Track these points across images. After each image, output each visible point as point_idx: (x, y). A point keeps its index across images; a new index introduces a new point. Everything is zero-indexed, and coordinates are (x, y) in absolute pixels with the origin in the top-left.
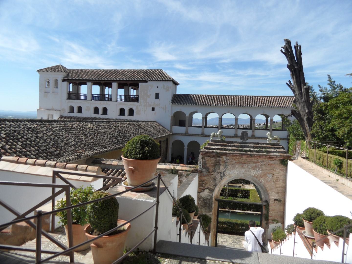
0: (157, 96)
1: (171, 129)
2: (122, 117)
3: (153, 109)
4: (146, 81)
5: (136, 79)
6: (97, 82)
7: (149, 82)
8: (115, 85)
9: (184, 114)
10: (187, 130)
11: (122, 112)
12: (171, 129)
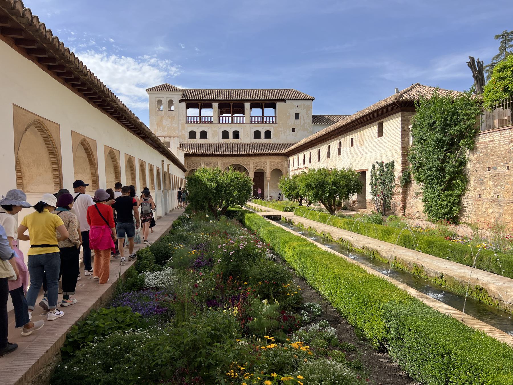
0: (297, 116)
2: (257, 141)
3: (294, 130)
4: (284, 101)
5: (273, 98)
6: (193, 102)
8: (247, 105)
11: (257, 135)
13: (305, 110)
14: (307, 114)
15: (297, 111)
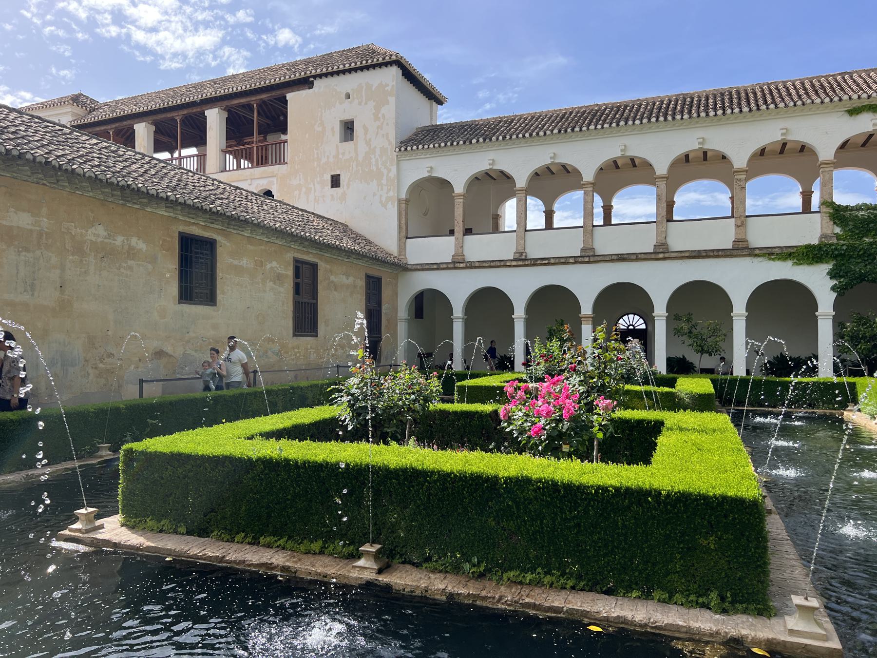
1: (402, 248)
3: (335, 181)
7: (317, 83)
9: (445, 184)
10: (460, 246)
12: (402, 248)
13: (372, 104)
14: (376, 118)
15: (346, 111)
